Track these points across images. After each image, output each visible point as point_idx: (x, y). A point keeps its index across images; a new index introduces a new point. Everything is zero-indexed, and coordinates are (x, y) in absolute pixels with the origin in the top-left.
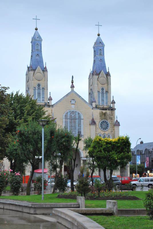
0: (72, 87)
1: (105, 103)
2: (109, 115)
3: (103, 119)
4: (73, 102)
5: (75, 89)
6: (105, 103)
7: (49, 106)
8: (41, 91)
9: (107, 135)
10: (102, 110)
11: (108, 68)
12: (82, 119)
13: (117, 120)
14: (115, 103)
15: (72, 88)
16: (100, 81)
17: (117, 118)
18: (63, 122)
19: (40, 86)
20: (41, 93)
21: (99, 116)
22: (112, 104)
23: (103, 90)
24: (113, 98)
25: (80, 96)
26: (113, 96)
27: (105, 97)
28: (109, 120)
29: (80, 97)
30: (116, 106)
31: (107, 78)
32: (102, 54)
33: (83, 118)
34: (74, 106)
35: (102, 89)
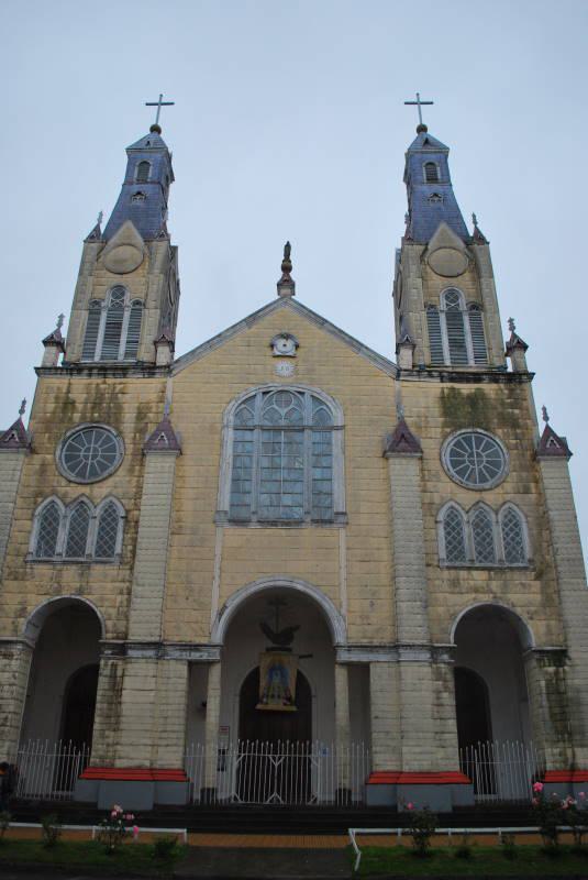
0: (286, 284)
1: (470, 354)
2: (499, 406)
3: (460, 428)
4: (283, 346)
5: (302, 296)
6: (470, 354)
7: (150, 369)
8: (127, 314)
9: (497, 513)
10: (452, 380)
11: (474, 216)
12: (338, 428)
13: (548, 429)
14: (525, 347)
15: (285, 291)
16: (432, 263)
17: (546, 418)
18: (222, 446)
19: (123, 294)
20: (125, 326)
21: (436, 410)
22: (509, 360)
23: (452, 301)
24: (512, 328)
25: (327, 321)
26: (511, 321)
27: (467, 327)
28: (500, 432)
29: (322, 322)
30: (532, 360)
31: (471, 251)
32: (439, 176)
33: (340, 423)
34: (291, 369)
35: (447, 298)
